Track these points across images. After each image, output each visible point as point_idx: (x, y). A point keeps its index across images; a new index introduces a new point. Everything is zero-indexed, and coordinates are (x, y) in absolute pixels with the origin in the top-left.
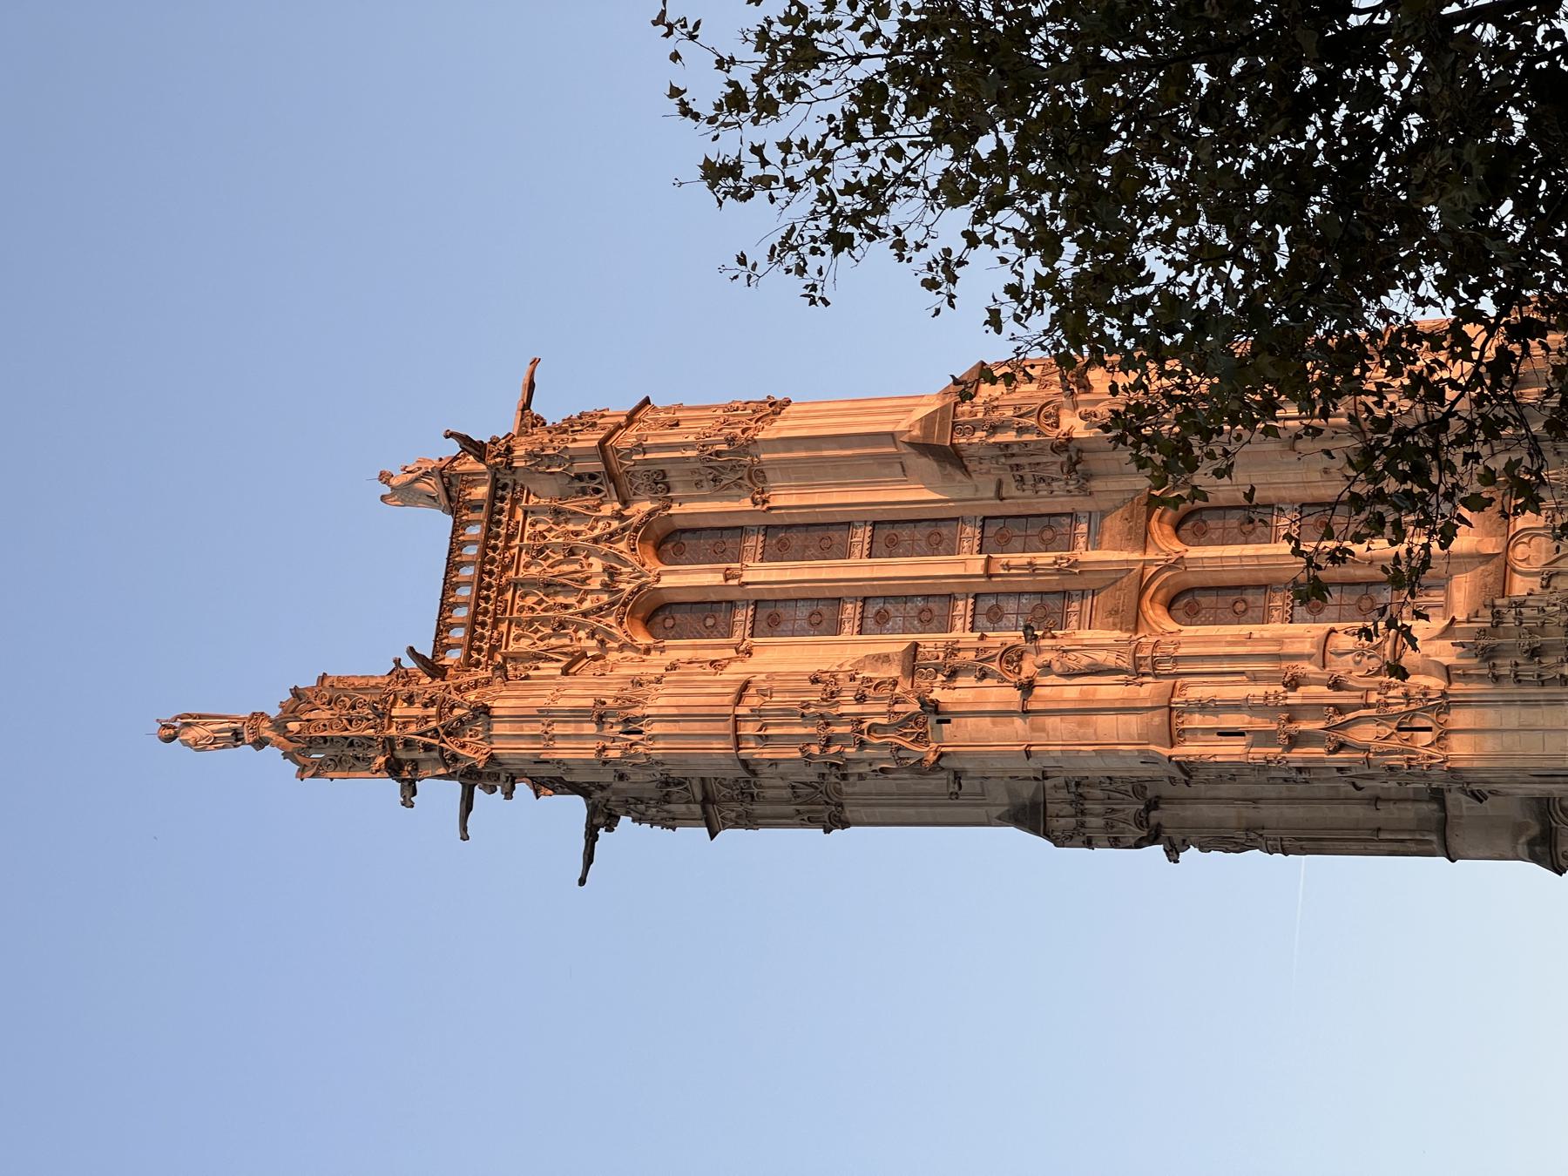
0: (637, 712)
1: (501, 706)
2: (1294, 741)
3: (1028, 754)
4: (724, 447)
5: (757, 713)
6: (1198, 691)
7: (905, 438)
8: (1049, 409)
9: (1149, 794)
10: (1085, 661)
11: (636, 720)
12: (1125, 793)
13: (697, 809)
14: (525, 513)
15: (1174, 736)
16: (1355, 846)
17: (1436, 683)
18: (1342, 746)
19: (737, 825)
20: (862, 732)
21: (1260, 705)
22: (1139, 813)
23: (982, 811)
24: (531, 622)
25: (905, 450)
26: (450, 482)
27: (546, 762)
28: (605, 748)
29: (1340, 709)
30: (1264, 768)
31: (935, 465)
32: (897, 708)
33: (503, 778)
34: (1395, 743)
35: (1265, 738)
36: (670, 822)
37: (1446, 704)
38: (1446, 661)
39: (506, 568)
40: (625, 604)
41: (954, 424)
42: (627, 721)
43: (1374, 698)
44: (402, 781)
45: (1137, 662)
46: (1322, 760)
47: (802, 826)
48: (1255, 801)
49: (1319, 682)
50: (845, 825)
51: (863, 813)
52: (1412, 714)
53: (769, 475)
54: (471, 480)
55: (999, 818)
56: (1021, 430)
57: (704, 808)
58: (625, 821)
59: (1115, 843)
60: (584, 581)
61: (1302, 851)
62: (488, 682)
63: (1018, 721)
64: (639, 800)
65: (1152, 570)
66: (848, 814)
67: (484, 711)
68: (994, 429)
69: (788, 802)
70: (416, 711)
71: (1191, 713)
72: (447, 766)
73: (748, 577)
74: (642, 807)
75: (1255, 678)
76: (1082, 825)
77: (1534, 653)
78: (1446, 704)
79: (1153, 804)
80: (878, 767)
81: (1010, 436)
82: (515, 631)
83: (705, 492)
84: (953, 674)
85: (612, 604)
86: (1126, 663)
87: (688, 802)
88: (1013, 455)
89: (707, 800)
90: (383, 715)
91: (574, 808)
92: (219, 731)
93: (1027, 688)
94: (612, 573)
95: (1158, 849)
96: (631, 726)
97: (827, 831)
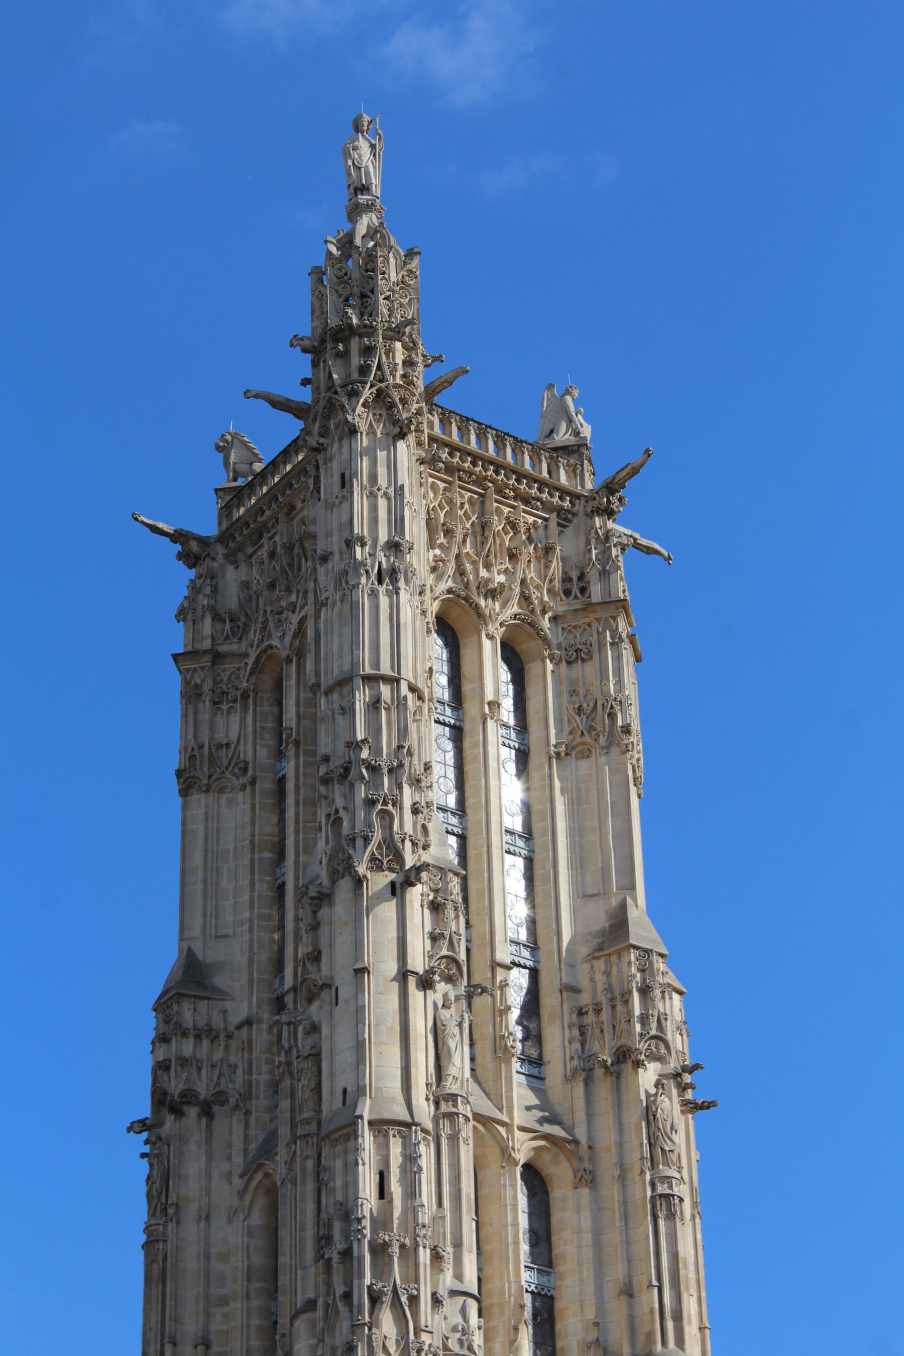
0: (402, 584)
2: (380, 1251)
3: (361, 971)
4: (620, 723)
5: (400, 703)
6: (426, 1155)
7: (629, 901)
8: (663, 1051)
9: (216, 1108)
10: (452, 1044)
11: (394, 580)
12: (218, 1084)
13: (207, 644)
14: (546, 519)
16: (155, 1318)
19: (186, 683)
20: (385, 803)
21: (415, 1218)
22: (196, 1095)
23: (197, 932)
24: (450, 502)
25: (614, 902)
26: (573, 452)
28: (363, 545)
29: (414, 1300)
30: (348, 1213)
31: (596, 928)
32: (408, 844)
33: (322, 440)
35: (382, 1222)
39: (499, 491)
40: (466, 599)
41: (648, 952)
42: (393, 573)
44: (323, 341)
45: (452, 1098)
46: (361, 1276)
49: (435, 1284)
50: (185, 792)
53: (584, 764)
54: (575, 471)
55: (190, 950)
56: (644, 1019)
57: (205, 652)
59: (162, 1067)
60: (488, 566)
63: (392, 967)
64: (215, 590)
65: (502, 1130)
66: (195, 797)
68: (645, 991)
69: (212, 738)
71: (404, 1146)
72: (344, 386)
74: (208, 590)
76: (185, 1034)
79: (207, 1111)
80: (342, 813)
83: (565, 699)
84: (436, 907)
85: (467, 586)
86: (451, 1086)
87: (213, 638)
88: (613, 1007)
89: (217, 657)
90: (395, 333)
92: (367, 174)
95: (144, 1110)
96: (389, 576)
97: (179, 773)
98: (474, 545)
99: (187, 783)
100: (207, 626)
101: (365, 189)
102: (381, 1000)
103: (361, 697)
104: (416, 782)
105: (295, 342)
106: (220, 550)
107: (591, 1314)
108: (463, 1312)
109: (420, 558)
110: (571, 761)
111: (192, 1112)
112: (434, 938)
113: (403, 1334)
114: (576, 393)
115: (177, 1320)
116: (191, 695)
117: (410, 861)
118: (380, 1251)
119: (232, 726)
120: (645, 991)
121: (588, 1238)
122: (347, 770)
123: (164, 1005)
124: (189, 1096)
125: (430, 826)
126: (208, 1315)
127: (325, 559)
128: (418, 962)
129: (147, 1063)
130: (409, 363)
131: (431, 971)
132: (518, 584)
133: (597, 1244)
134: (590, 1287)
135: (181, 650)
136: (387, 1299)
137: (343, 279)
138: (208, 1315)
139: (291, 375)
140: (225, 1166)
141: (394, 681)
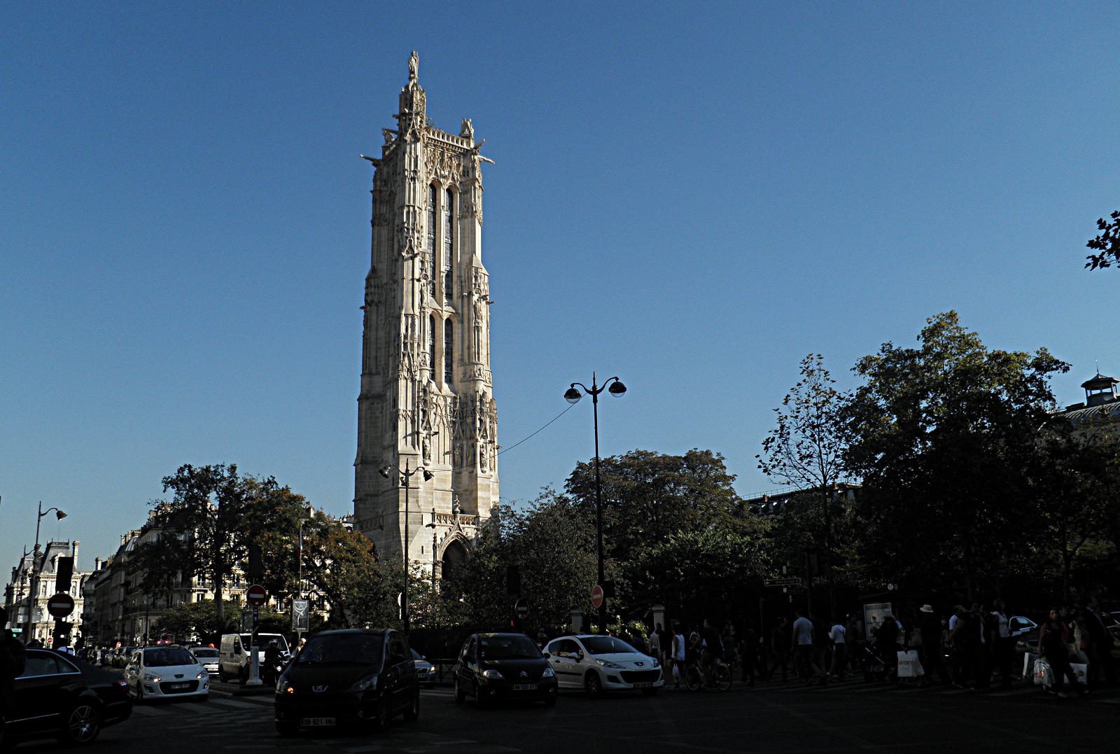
0: (417, 181)
1: (418, 144)
2: (405, 344)
5: (415, 211)
11: (415, 181)
13: (378, 188)
15: (406, 316)
17: (418, 378)
18: (404, 355)
27: (404, 155)
29: (413, 355)
30: (399, 334)
34: (405, 368)
36: (375, 180)
37: (413, 381)
38: (423, 380)
39: (447, 150)
43: (415, 363)
45: (424, 308)
47: (373, 215)
48: (377, 330)
50: (373, 226)
51: (376, 232)
52: (411, 372)
53: (466, 220)
56: (475, 284)
58: (375, 169)
59: (366, 295)
61: (364, 340)
62: (424, 142)
64: (381, 174)
67: (417, 140)
68: (476, 277)
69: (379, 212)
70: (419, 123)
73: (442, 211)
75: (419, 336)
77: (425, 401)
78: (413, 381)
79: (377, 305)
81: (474, 282)
82: (432, 150)
84: (422, 262)
85: (438, 176)
86: (424, 305)
89: (380, 191)
90: (417, 114)
91: (379, 156)
93: (419, 280)
94: (444, 177)
96: (413, 179)
97: (371, 222)
98: (440, 165)
99: (373, 223)
100: (379, 183)
101: (413, 73)
102: (407, 285)
103: (405, 210)
104: (418, 232)
105: (394, 116)
106: (382, 163)
107: (460, 353)
108: (425, 357)
109: (422, 174)
110: (463, 220)
111: (374, 305)
112: (422, 270)
113: (410, 364)
114: (470, 120)
115: (370, 353)
116: (374, 201)
117: (416, 252)
118: (405, 344)
119: (384, 209)
120: (476, 277)
121: (460, 335)
122: (402, 229)
123: (367, 280)
124: (372, 301)
125: (422, 243)
126: (377, 352)
127: (399, 174)
128: (417, 276)
129: (364, 292)
130: (421, 122)
131: (420, 278)
132: (450, 175)
133: (463, 337)
134: (460, 347)
135: (372, 189)
136: (407, 355)
137: (406, 99)
138: (377, 352)
139: (394, 125)
140: (381, 317)
141: (414, 207)
